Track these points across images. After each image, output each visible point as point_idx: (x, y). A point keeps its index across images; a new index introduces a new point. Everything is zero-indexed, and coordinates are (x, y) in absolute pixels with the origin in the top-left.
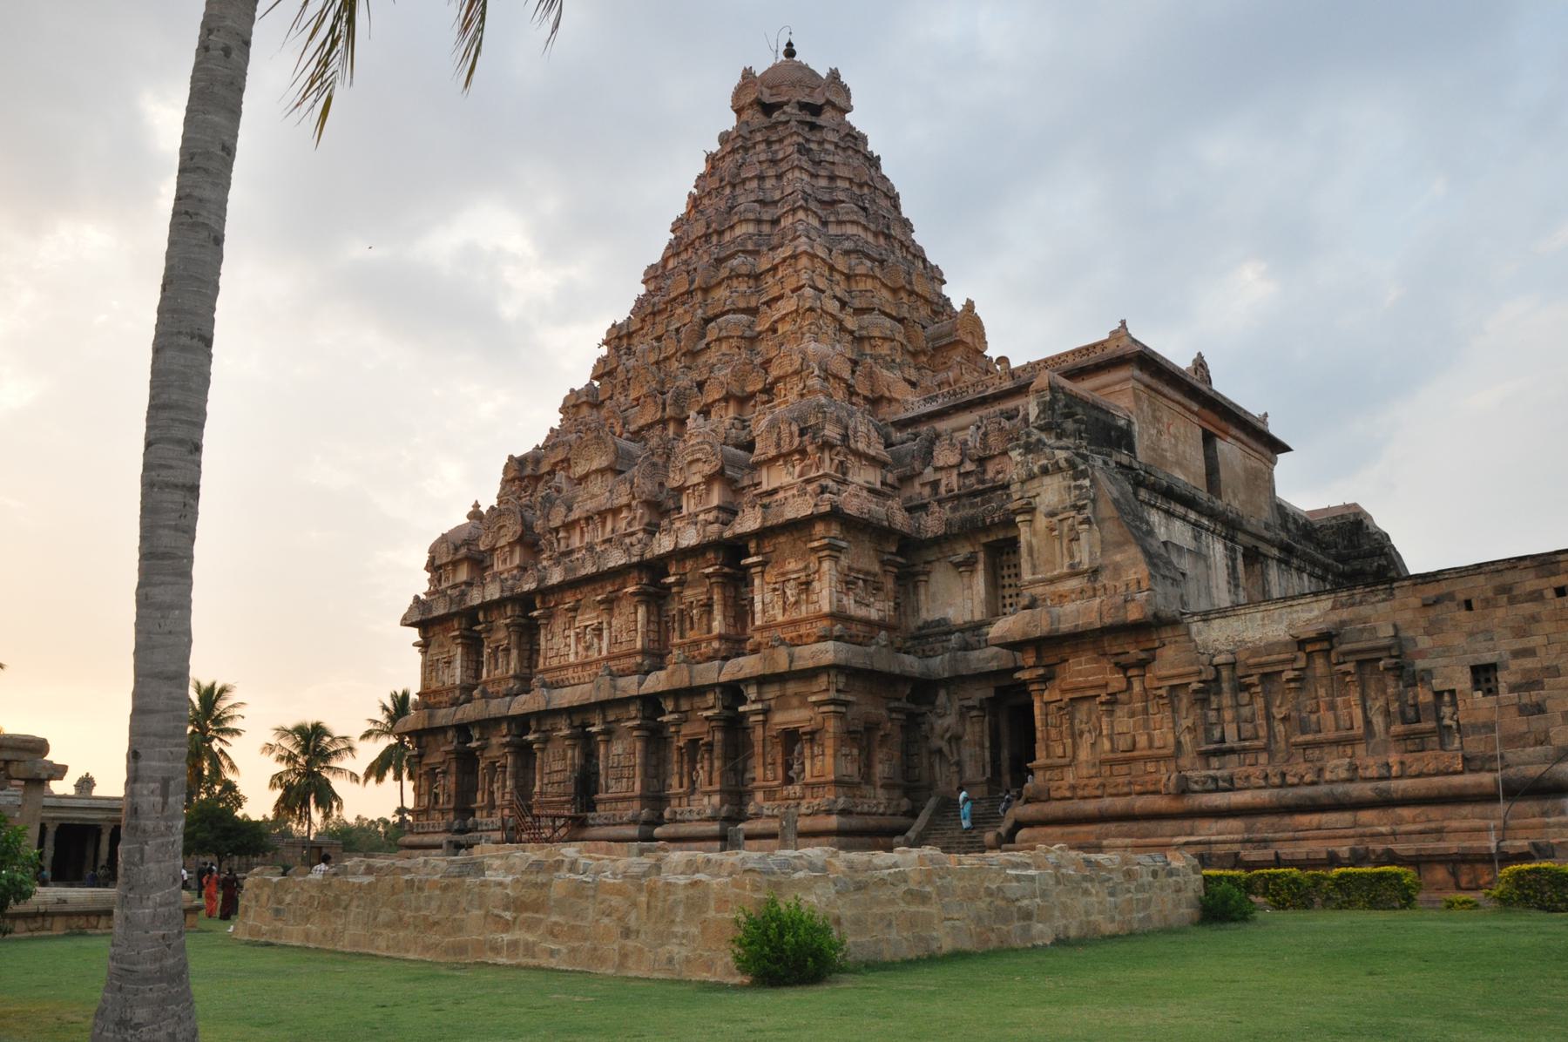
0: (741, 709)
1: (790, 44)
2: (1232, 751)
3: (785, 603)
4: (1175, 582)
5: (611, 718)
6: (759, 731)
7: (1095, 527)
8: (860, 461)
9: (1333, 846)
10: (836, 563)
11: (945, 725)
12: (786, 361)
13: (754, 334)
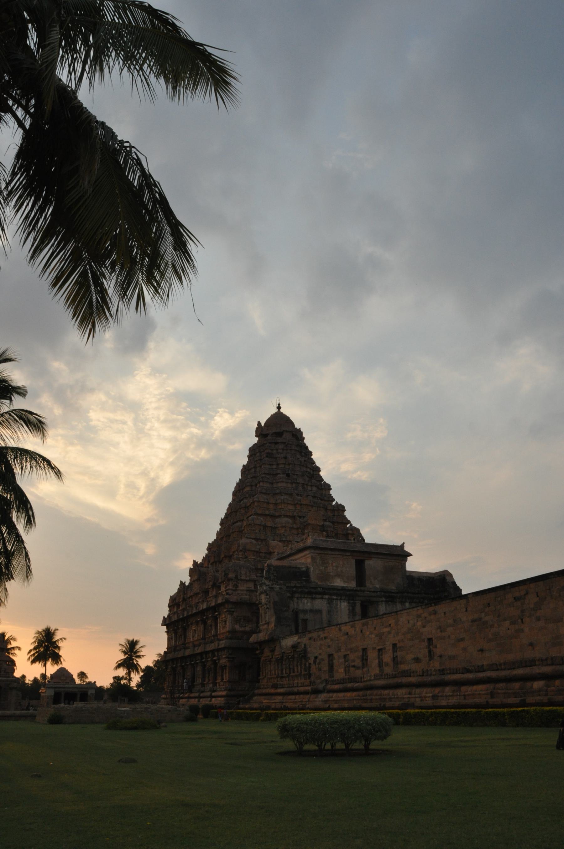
0: (214, 658)
1: (279, 404)
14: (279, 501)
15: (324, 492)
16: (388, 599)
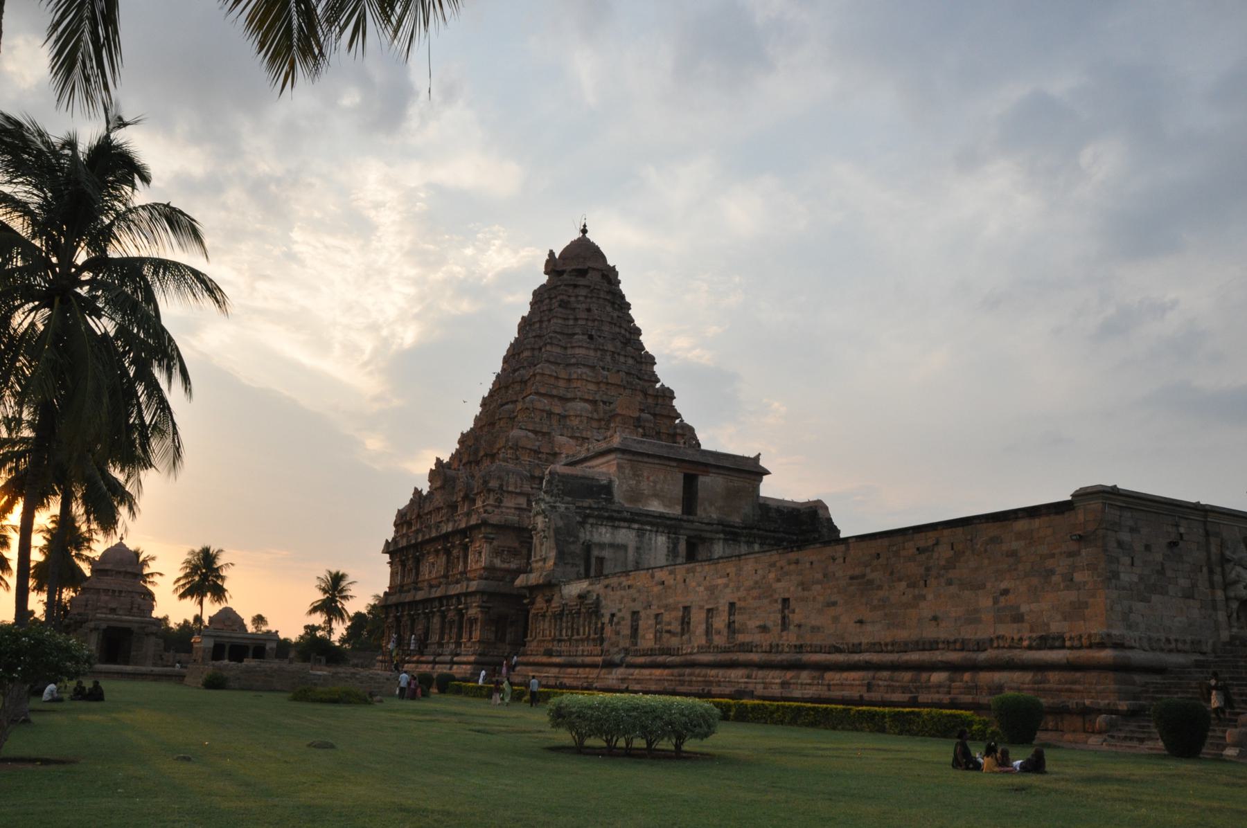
0: (460, 607)
14: (575, 376)
15: (644, 368)
16: (728, 537)
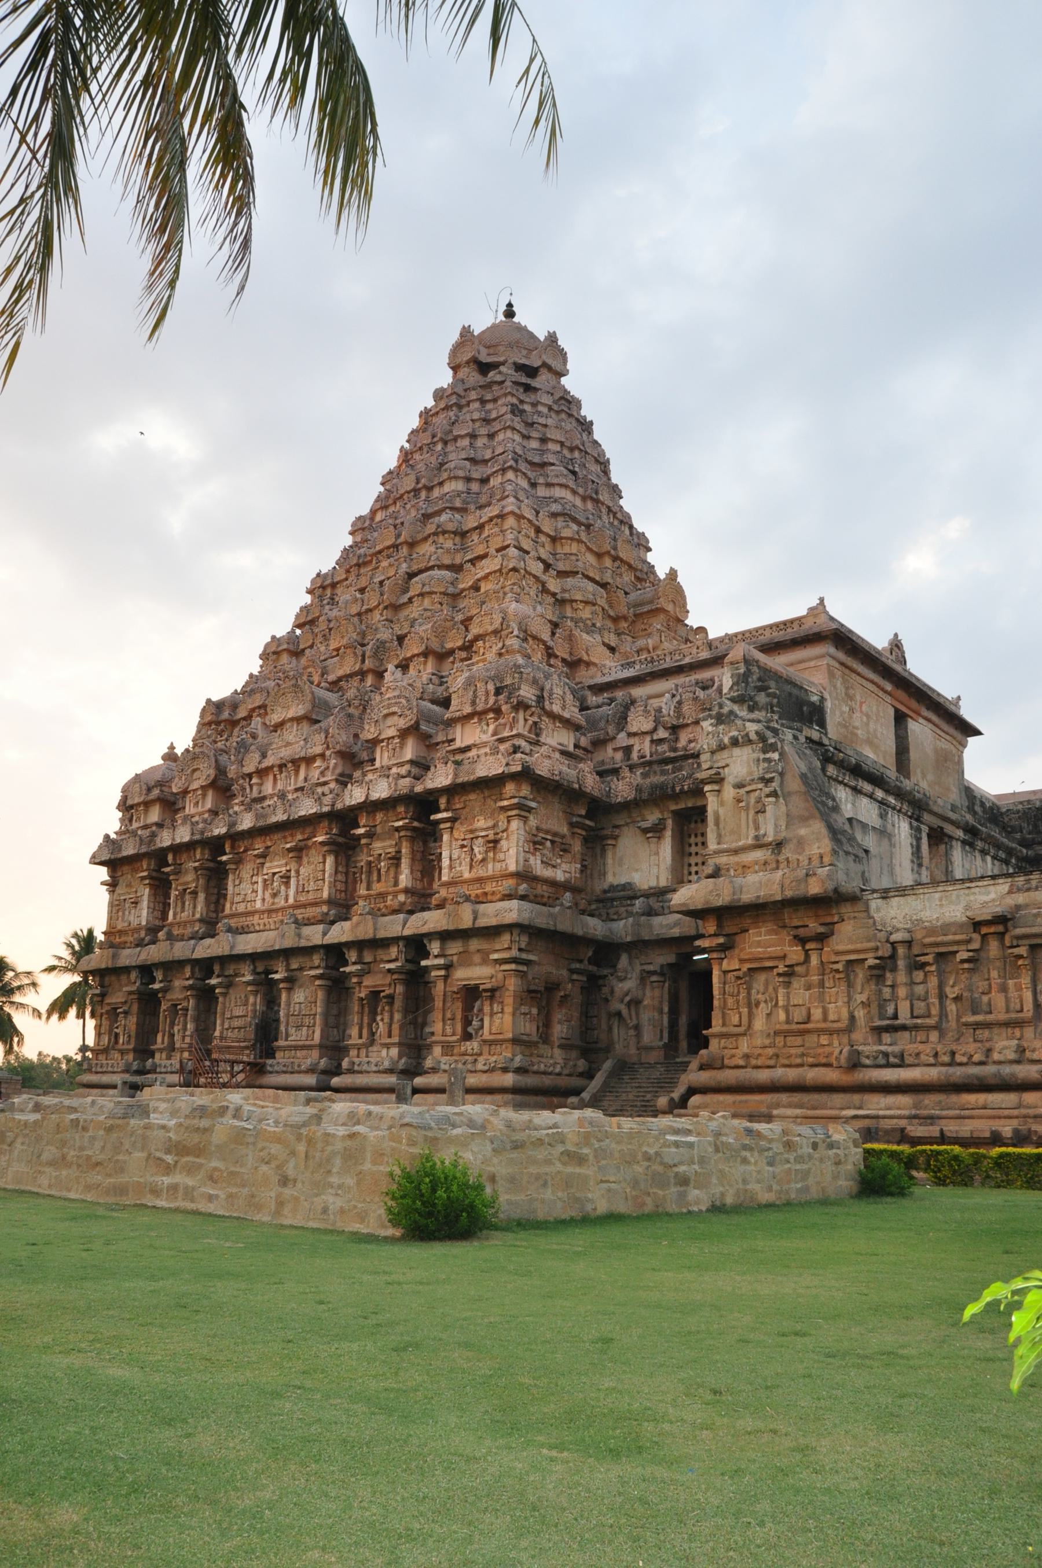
0: (424, 963)
1: (510, 305)
2: (904, 1028)
3: (472, 860)
4: (857, 858)
5: (294, 966)
6: (440, 986)
7: (781, 800)
8: (554, 723)
9: (998, 1125)
10: (525, 823)
11: (625, 989)
12: (487, 620)
13: (457, 591)
